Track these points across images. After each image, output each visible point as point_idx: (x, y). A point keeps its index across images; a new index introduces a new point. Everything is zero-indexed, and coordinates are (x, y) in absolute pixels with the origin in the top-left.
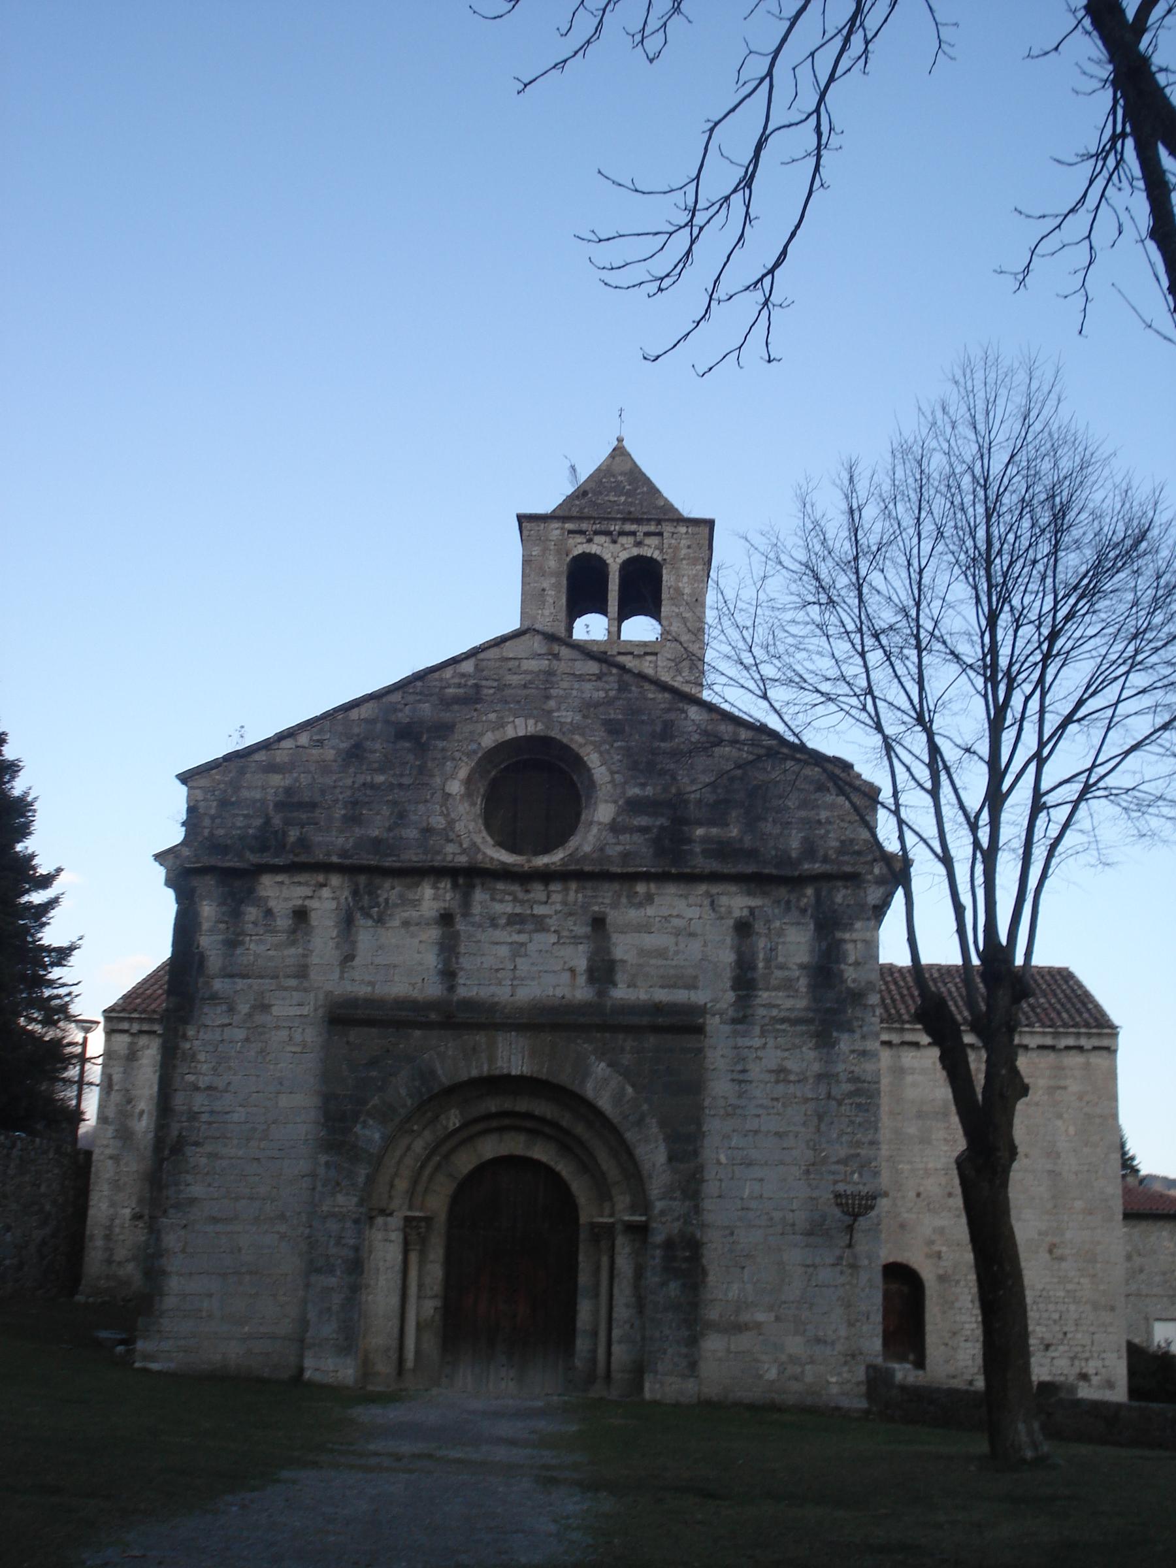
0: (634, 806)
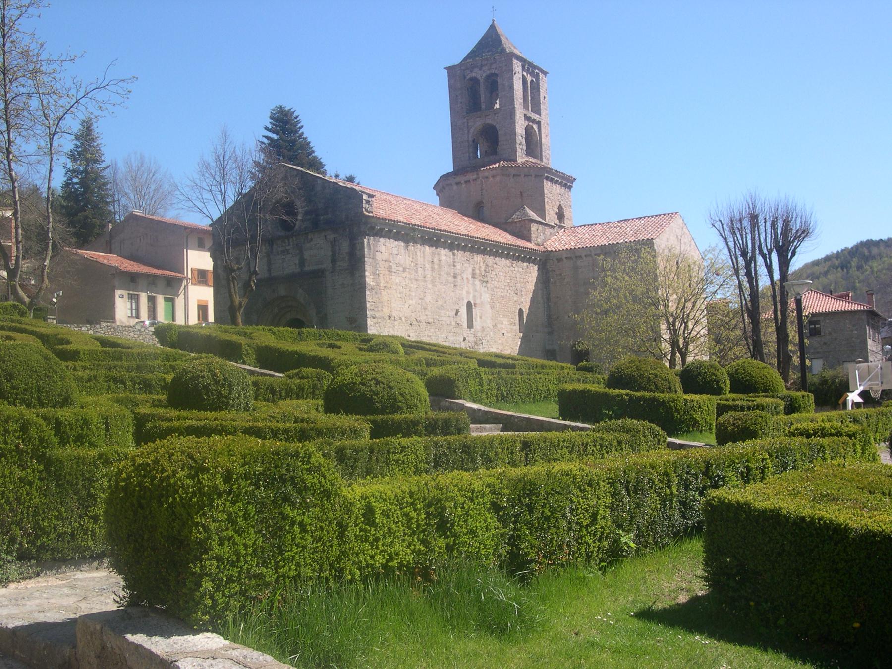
0: (307, 213)
